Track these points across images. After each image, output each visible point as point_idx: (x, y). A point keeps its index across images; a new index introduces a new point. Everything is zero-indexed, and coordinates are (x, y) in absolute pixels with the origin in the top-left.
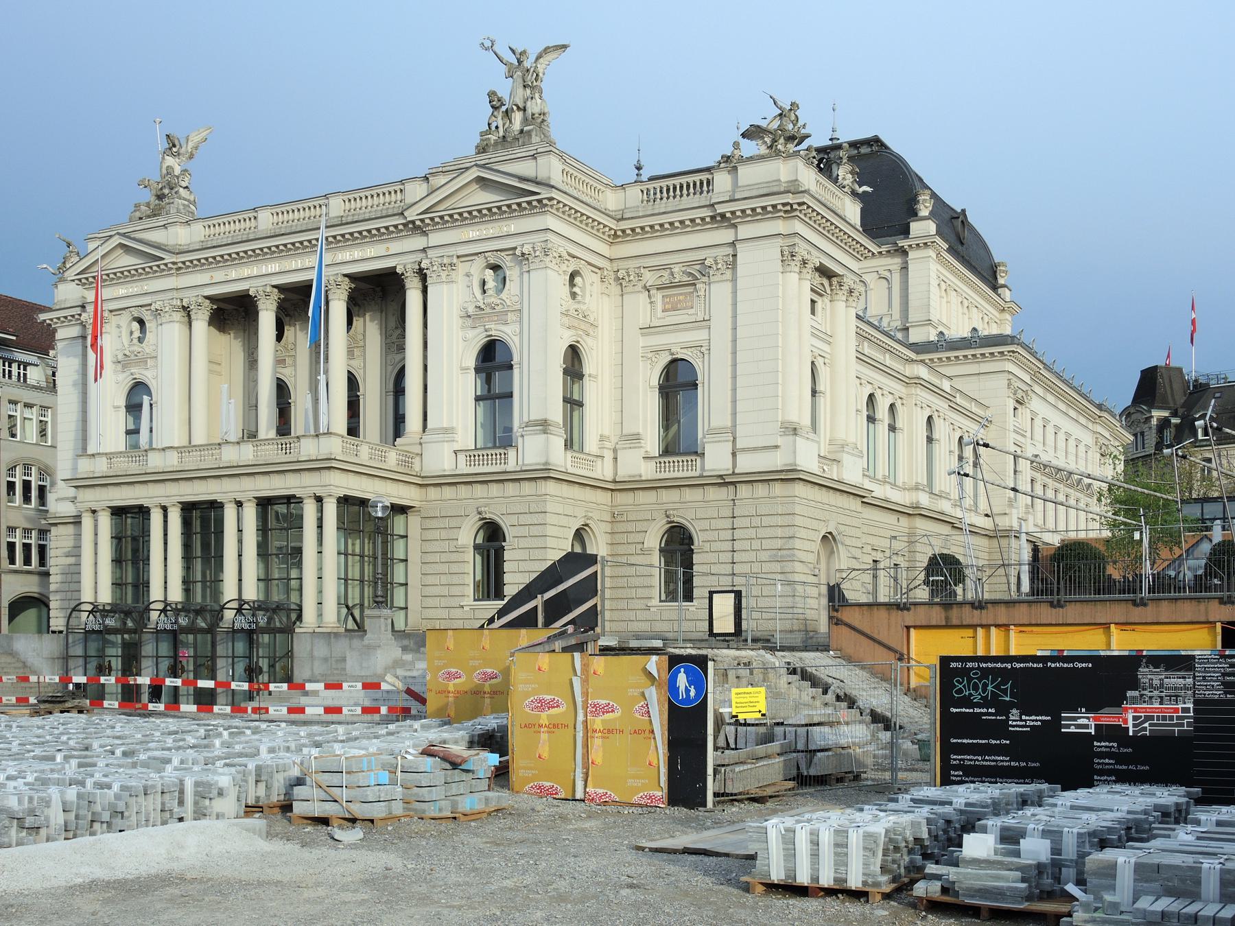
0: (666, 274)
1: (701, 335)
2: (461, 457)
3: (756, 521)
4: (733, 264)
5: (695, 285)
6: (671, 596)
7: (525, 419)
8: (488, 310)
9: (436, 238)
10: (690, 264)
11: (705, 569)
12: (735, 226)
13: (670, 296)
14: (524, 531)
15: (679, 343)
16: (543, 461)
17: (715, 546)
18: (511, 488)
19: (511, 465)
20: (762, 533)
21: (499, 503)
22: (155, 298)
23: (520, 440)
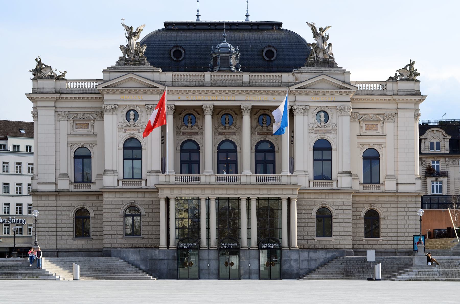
2: (312, 183)
3: (406, 210)
4: (395, 116)
6: (368, 234)
7: (340, 170)
8: (323, 128)
9: (298, 98)
11: (385, 226)
13: (368, 125)
14: (341, 212)
16: (350, 186)
17: (389, 218)
19: (335, 187)
20: (409, 214)
22: (147, 103)
23: (339, 179)
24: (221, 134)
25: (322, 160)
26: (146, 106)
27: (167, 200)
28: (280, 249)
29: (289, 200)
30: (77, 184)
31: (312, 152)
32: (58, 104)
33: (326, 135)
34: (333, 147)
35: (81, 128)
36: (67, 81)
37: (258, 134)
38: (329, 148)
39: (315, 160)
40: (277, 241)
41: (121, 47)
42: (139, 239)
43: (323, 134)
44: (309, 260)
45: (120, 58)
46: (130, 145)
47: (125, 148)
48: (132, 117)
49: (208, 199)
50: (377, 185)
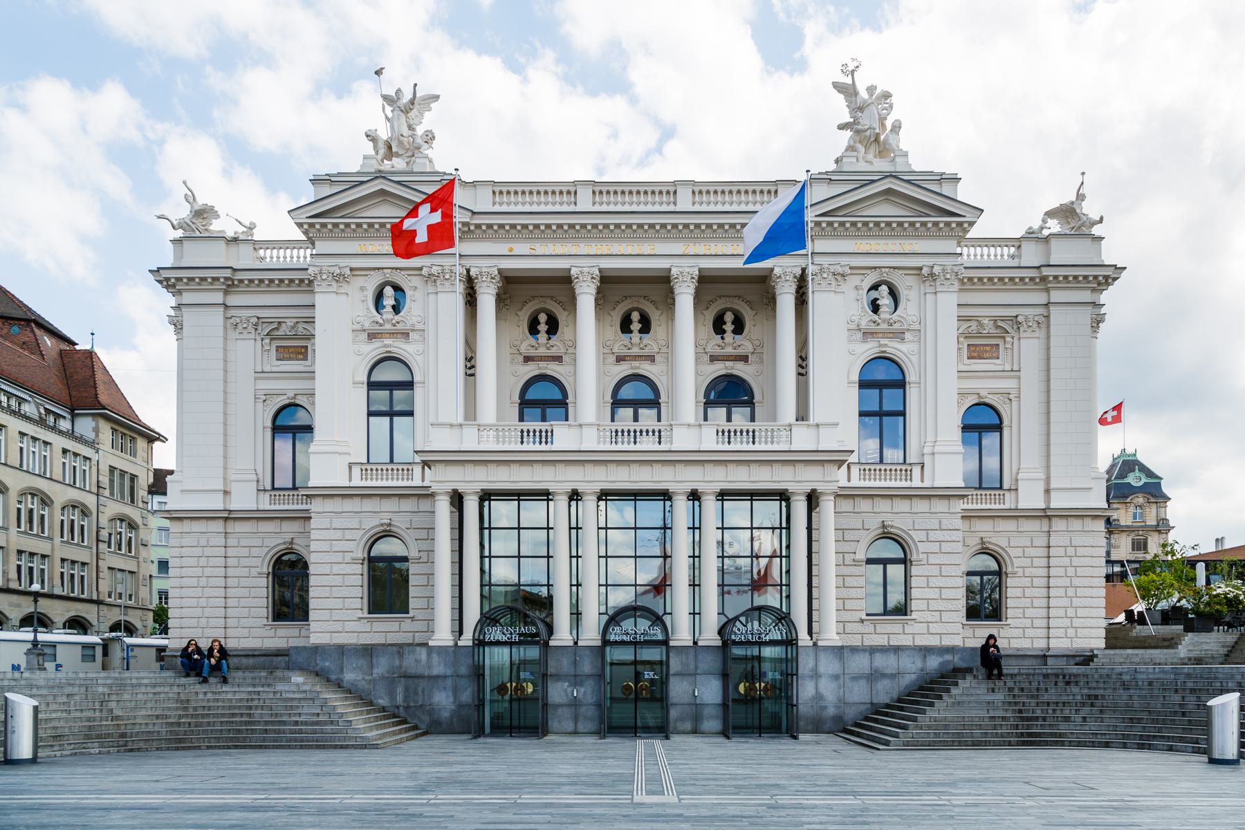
0: (974, 325)
1: (1009, 384)
5: (1004, 338)
10: (1004, 319)
12: (1047, 290)
13: (976, 346)
15: (987, 388)
18: (922, 506)
21: (900, 517)
24: (620, 359)
25: (881, 414)
26: (425, 271)
27: (457, 499)
28: (790, 642)
29: (812, 499)
30: (277, 493)
31: (855, 389)
32: (233, 300)
33: (890, 344)
34: (911, 377)
35: (290, 359)
36: (257, 245)
37: (713, 359)
38: (901, 384)
39: (862, 414)
40: (783, 618)
41: (372, 137)
42: (401, 620)
43: (883, 341)
44: (874, 676)
45: (365, 157)
46: (382, 375)
47: (372, 386)
48: (389, 301)
49: (575, 496)
50: (997, 492)
